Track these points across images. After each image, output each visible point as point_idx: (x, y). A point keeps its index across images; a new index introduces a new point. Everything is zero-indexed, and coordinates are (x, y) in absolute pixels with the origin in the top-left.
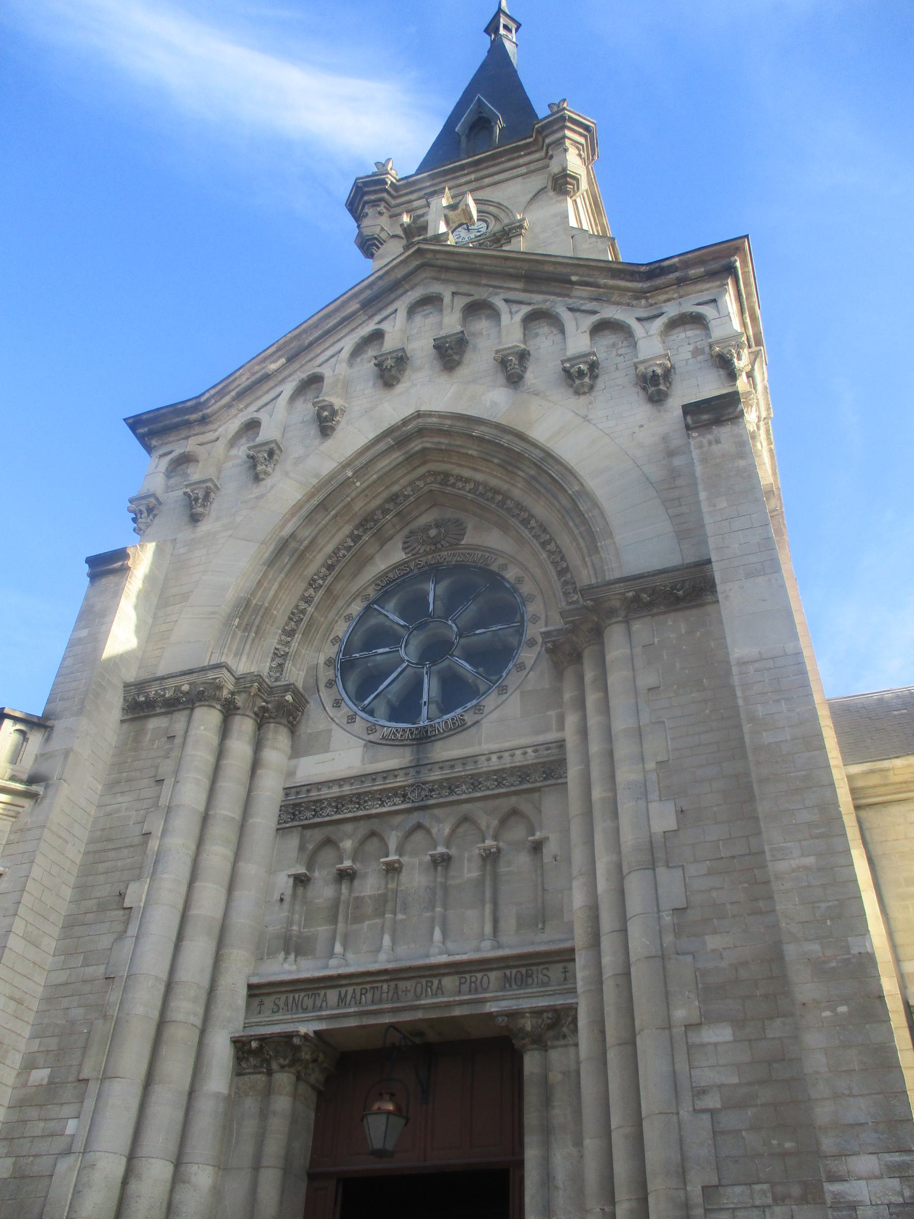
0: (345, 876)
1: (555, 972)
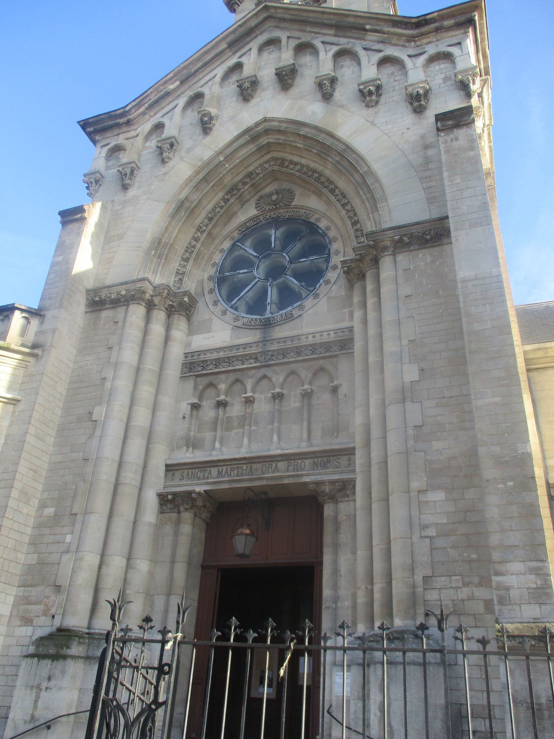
0: (222, 405)
1: (343, 460)
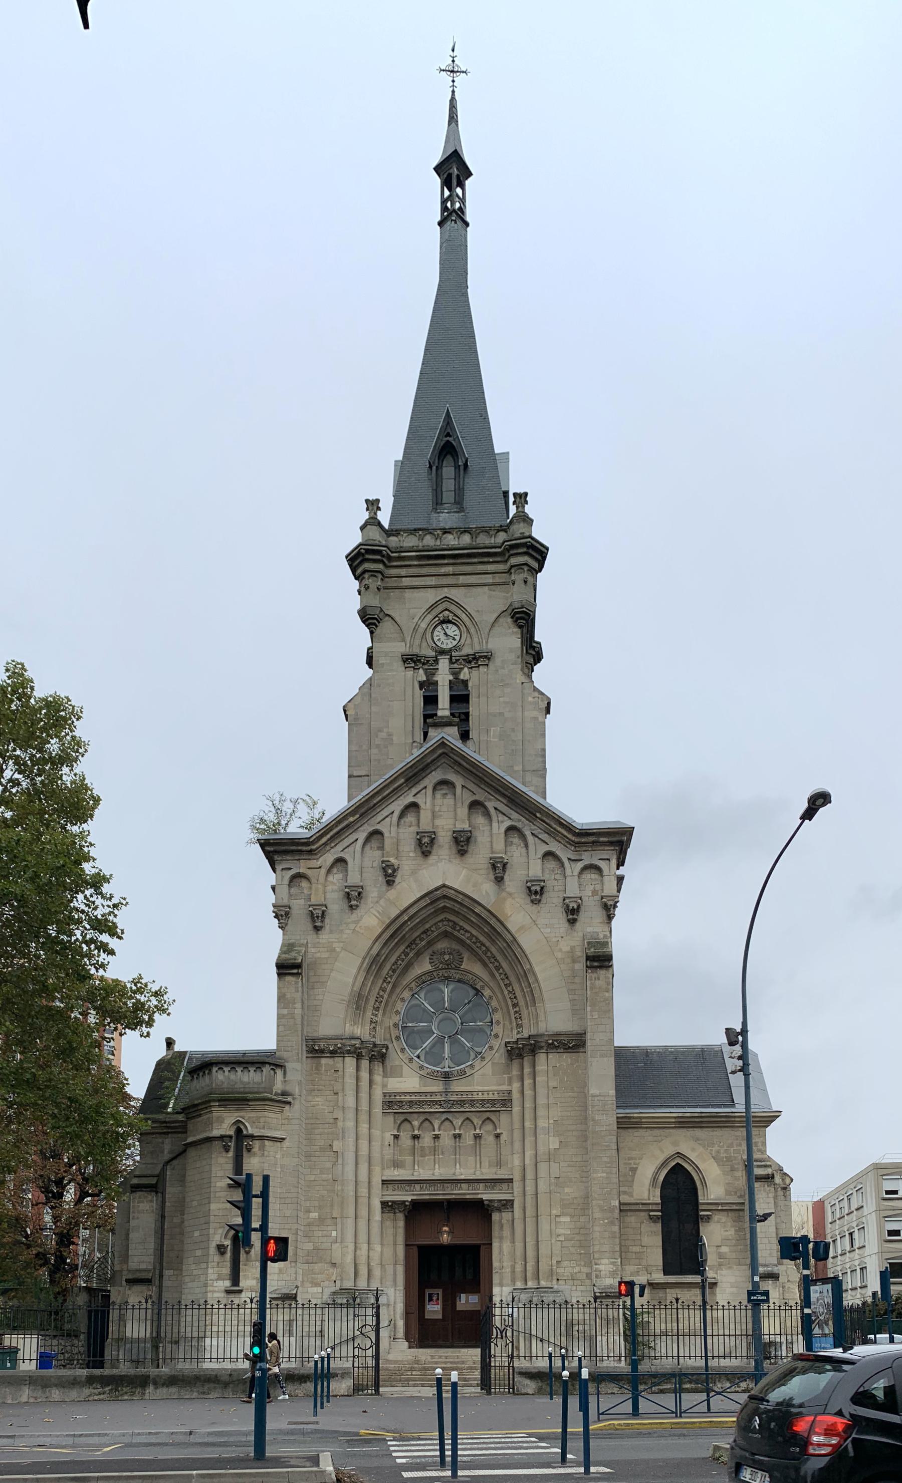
0: (415, 1137)
1: (505, 1186)
